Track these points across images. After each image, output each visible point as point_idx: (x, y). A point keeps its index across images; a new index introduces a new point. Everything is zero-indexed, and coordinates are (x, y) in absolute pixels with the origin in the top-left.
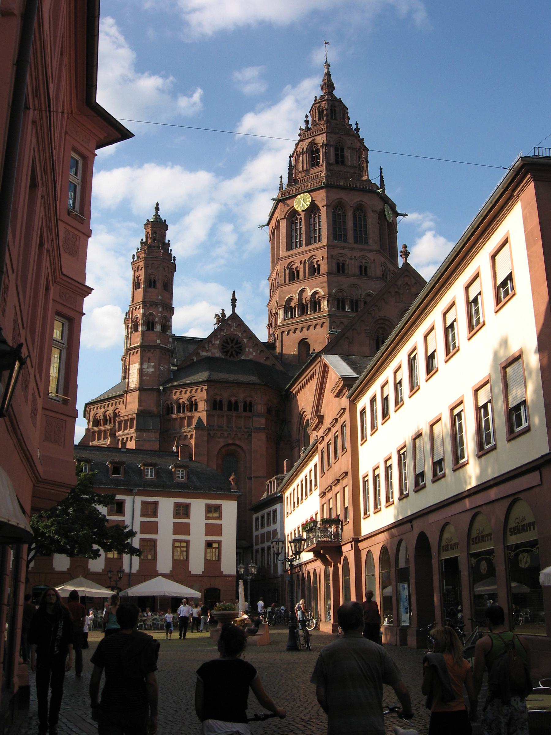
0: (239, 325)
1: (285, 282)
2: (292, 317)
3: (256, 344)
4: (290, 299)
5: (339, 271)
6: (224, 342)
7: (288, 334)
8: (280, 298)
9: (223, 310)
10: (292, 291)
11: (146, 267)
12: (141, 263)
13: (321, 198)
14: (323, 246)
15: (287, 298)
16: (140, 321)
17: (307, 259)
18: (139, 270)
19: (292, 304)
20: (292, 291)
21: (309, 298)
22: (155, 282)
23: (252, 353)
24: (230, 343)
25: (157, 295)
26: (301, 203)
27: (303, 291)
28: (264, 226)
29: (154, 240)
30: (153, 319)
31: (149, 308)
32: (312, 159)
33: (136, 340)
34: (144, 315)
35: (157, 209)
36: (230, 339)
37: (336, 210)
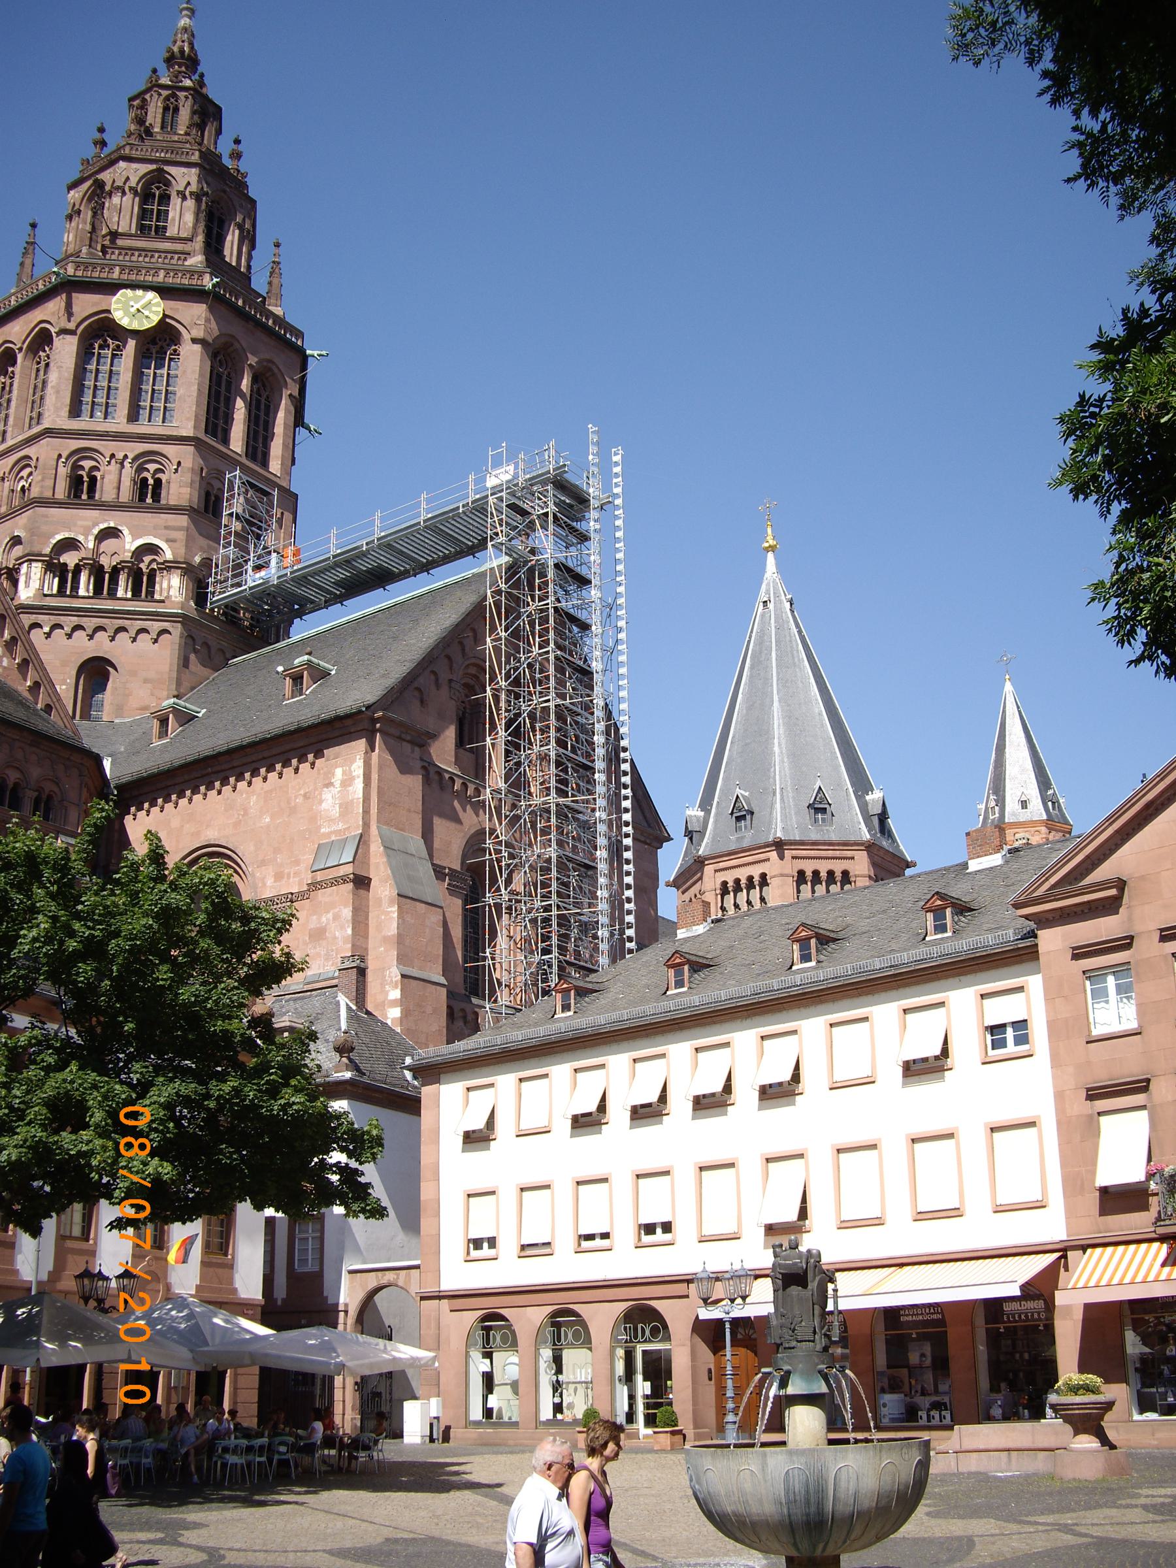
2: (61, 592)
4: (70, 544)
5: (206, 510)
7: (48, 635)
15: (59, 537)
17: (131, 456)
21: (127, 556)
32: (144, 214)
37: (223, 359)
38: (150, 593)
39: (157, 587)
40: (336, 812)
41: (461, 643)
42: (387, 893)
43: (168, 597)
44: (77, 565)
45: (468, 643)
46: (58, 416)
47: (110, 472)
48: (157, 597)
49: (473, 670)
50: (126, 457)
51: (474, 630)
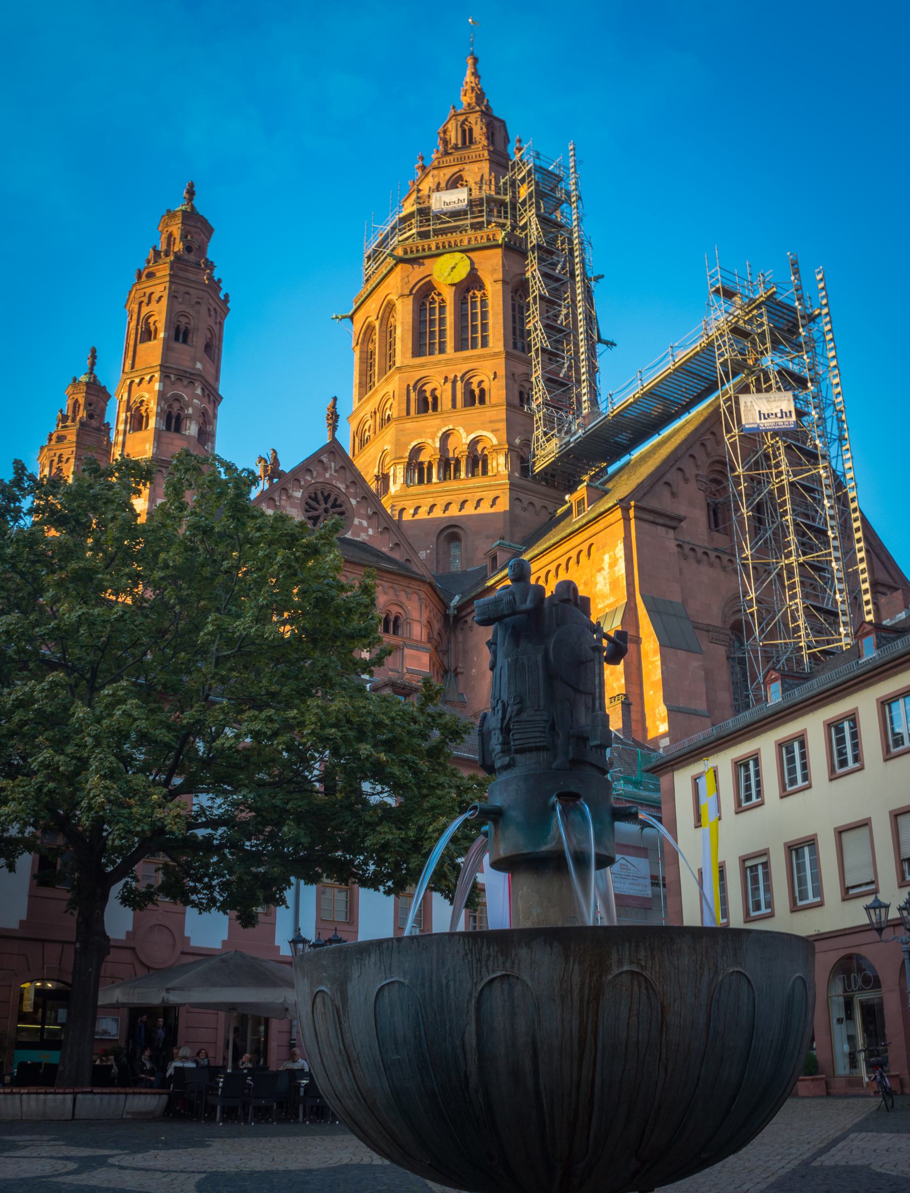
0: (342, 467)
1: (408, 413)
2: (421, 481)
3: (375, 513)
6: (310, 497)
8: (398, 444)
9: (274, 451)
10: (427, 434)
11: (172, 297)
12: (161, 288)
13: (491, 266)
14: (496, 354)
15: (413, 444)
16: (153, 406)
17: (459, 375)
18: (153, 302)
19: (424, 458)
20: (427, 434)
22: (186, 333)
23: (365, 530)
24: (322, 502)
25: (190, 358)
26: (447, 271)
27: (446, 436)
28: (343, 318)
29: (188, 249)
30: (182, 409)
31: (173, 383)
33: (138, 448)
34: (161, 395)
35: (191, 193)
36: (322, 493)
38: (485, 472)
39: (490, 467)
40: (607, 589)
41: (703, 445)
42: (651, 646)
43: (498, 472)
44: (430, 462)
45: (710, 445)
46: (405, 358)
47: (446, 390)
48: (490, 474)
49: (718, 467)
50: (456, 376)
51: (713, 433)
